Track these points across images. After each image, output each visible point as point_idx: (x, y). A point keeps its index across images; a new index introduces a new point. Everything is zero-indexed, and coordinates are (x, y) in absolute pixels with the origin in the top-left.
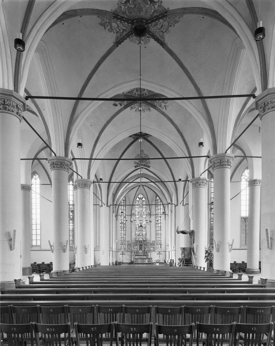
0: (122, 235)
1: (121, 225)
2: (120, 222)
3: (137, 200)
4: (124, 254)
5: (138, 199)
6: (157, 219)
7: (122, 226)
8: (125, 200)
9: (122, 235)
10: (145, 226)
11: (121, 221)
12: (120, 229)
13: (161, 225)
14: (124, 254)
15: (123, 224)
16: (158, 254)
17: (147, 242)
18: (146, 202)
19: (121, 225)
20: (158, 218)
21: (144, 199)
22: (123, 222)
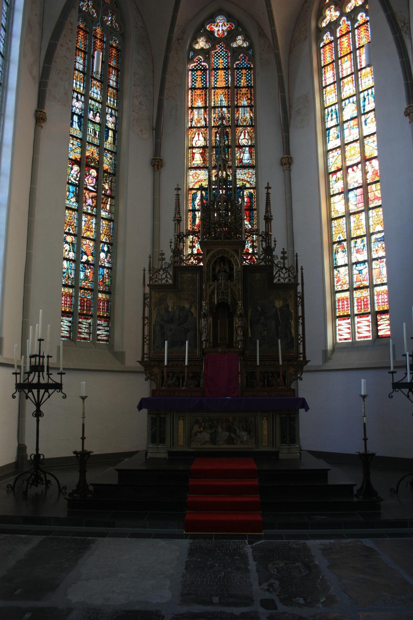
0: (88, 245)
1: (83, 174)
2: (75, 154)
3: (197, 47)
4: (58, 386)
5: (202, 44)
6: (333, 143)
7: (90, 182)
8: (123, 36)
9: (88, 245)
10: (250, 196)
11: (83, 148)
12: (75, 205)
13: (365, 173)
14: (58, 386)
15: (94, 172)
16: (397, 386)
17: (281, 277)
18: (252, 59)
19: (83, 174)
20: (341, 136)
21: (240, 42)
22: (100, 162)
